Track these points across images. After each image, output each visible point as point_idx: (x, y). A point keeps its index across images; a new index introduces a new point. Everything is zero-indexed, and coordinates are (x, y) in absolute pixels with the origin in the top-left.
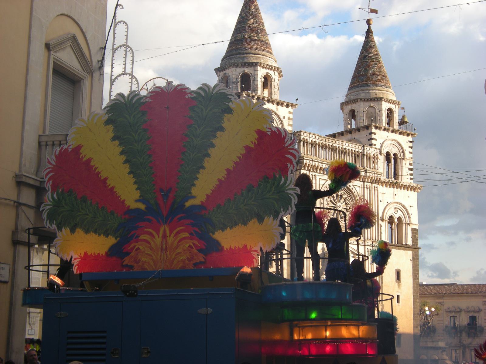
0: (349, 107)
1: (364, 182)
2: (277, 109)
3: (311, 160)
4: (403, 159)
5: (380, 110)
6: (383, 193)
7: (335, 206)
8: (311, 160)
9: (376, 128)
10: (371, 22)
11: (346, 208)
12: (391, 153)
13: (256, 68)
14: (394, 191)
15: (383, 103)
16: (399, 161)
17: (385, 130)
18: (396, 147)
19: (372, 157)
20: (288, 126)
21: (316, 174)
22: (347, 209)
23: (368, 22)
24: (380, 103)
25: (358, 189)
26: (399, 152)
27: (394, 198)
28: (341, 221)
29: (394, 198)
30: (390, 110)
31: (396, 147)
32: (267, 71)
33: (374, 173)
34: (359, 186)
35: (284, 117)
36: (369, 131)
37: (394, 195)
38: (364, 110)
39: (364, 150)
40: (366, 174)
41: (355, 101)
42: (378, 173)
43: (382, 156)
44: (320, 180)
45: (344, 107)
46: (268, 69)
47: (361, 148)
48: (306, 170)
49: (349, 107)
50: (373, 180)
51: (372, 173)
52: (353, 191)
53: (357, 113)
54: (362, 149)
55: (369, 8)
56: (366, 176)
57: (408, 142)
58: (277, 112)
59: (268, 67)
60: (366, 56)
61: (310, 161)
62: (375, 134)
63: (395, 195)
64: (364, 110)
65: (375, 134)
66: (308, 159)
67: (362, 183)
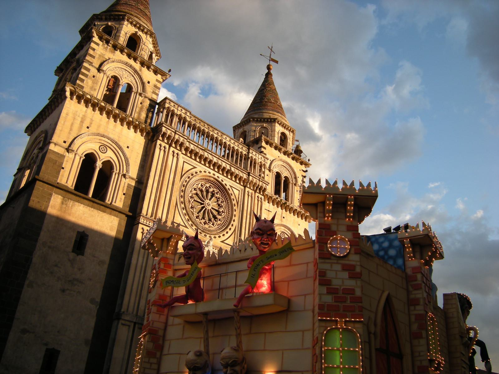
0: (241, 130)
1: (245, 187)
2: (141, 70)
3: (173, 132)
4: (295, 185)
5: (273, 131)
6: (269, 211)
7: (203, 202)
8: (173, 132)
9: (267, 143)
10: (271, 67)
11: (217, 209)
12: (282, 176)
13: (122, 22)
14: (282, 213)
15: (277, 124)
16: (290, 185)
17: (276, 148)
18: (288, 170)
19: (258, 164)
20: (152, 93)
21: (180, 153)
22: (219, 212)
23: (269, 68)
24: (273, 124)
25: (236, 192)
26: (290, 177)
27: (282, 221)
28: (209, 224)
29: (282, 221)
30: (283, 134)
31: (288, 170)
32: (137, 30)
33: (259, 179)
34: (239, 191)
35: (149, 82)
36: (259, 146)
37: (281, 217)
38: (255, 129)
39: (248, 153)
40: (248, 178)
41: (247, 121)
42: (263, 181)
43: (271, 173)
44: (185, 163)
45: (236, 132)
46: (139, 28)
47: (246, 150)
48: (166, 143)
49: (241, 130)
50: (257, 188)
51: (256, 179)
52: (230, 192)
53: (248, 132)
54: (247, 151)
55: (270, 57)
56: (249, 180)
57: (301, 170)
58: (140, 72)
59: (138, 25)
60: (264, 89)
61: (173, 133)
62: (265, 148)
63: (284, 218)
64: (255, 129)
65: (265, 148)
66: (170, 128)
67: (243, 188)
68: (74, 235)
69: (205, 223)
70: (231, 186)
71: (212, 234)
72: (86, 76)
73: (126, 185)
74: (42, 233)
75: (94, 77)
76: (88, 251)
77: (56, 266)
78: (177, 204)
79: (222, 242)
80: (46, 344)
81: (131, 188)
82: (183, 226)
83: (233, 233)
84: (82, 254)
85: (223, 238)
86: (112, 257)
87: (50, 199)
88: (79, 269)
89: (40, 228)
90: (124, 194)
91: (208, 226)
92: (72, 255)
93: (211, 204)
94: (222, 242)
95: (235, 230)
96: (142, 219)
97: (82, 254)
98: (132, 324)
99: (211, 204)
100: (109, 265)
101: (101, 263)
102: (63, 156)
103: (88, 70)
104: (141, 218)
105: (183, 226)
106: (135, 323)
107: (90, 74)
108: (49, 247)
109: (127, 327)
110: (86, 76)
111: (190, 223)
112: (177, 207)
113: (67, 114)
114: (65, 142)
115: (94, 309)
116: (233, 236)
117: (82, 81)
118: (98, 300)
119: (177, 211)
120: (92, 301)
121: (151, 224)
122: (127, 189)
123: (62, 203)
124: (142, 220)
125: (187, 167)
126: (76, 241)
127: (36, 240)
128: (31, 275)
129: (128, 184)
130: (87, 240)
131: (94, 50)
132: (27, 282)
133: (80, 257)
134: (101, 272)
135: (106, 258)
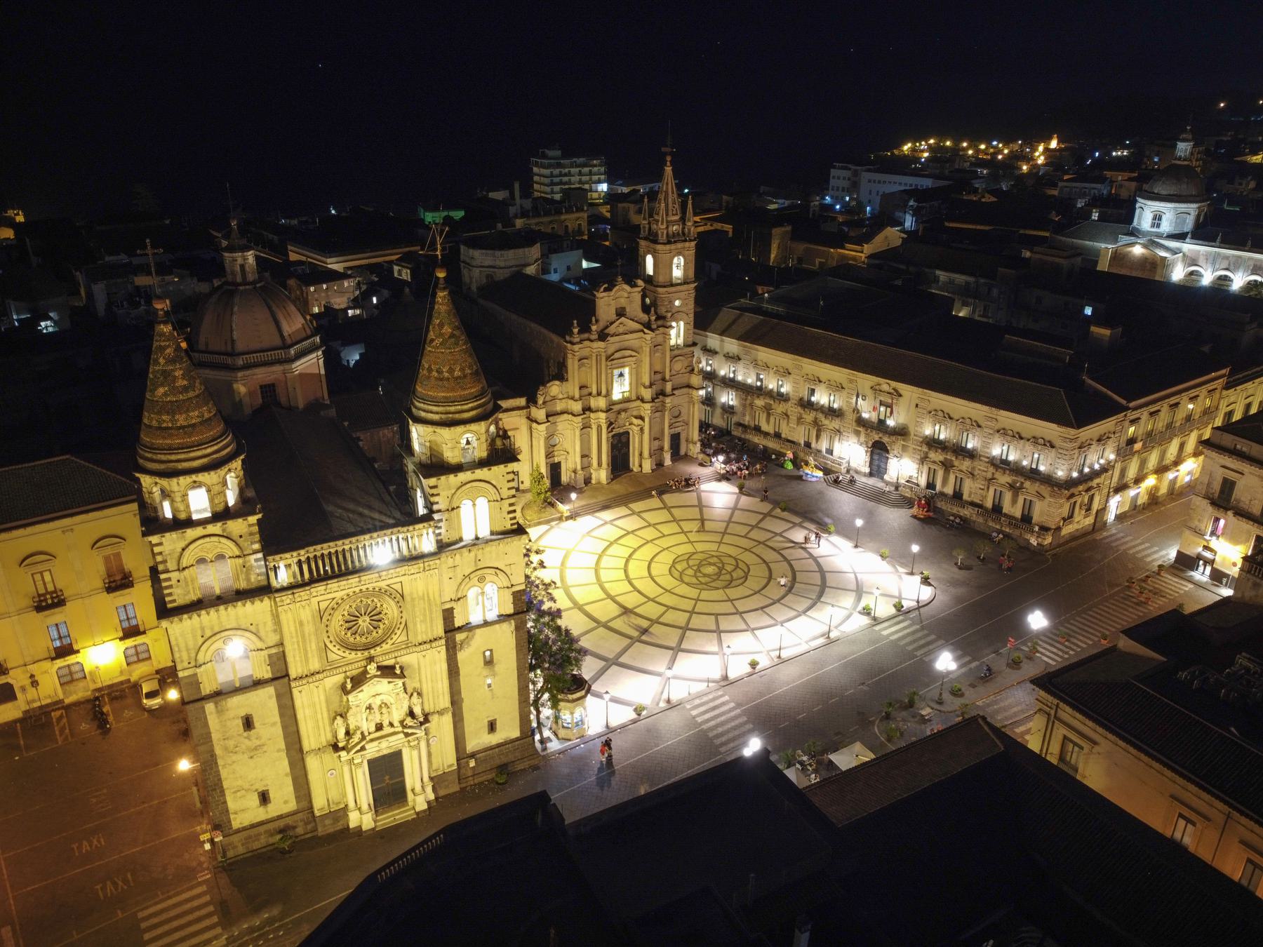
68: (240, 722)
70: (388, 586)
72: (170, 587)
73: (267, 657)
74: (213, 735)
75: (179, 581)
76: (257, 724)
77: (237, 747)
79: (393, 644)
80: (256, 790)
84: (254, 728)
86: (282, 715)
87: (204, 712)
88: (257, 738)
89: (210, 733)
92: (245, 734)
93: (364, 622)
97: (254, 728)
99: (364, 622)
100: (281, 722)
101: (274, 724)
102: (195, 675)
103: (169, 579)
107: (173, 582)
108: (224, 739)
110: (170, 587)
111: (348, 652)
113: (176, 640)
114: (189, 663)
115: (284, 754)
117: (170, 594)
118: (284, 747)
119: (329, 652)
120: (279, 751)
123: (216, 707)
125: (323, 605)
126: (243, 724)
127: (211, 741)
128: (220, 762)
130: (252, 718)
131: (161, 553)
132: (220, 768)
133: (253, 731)
134: (278, 731)
135: (277, 719)
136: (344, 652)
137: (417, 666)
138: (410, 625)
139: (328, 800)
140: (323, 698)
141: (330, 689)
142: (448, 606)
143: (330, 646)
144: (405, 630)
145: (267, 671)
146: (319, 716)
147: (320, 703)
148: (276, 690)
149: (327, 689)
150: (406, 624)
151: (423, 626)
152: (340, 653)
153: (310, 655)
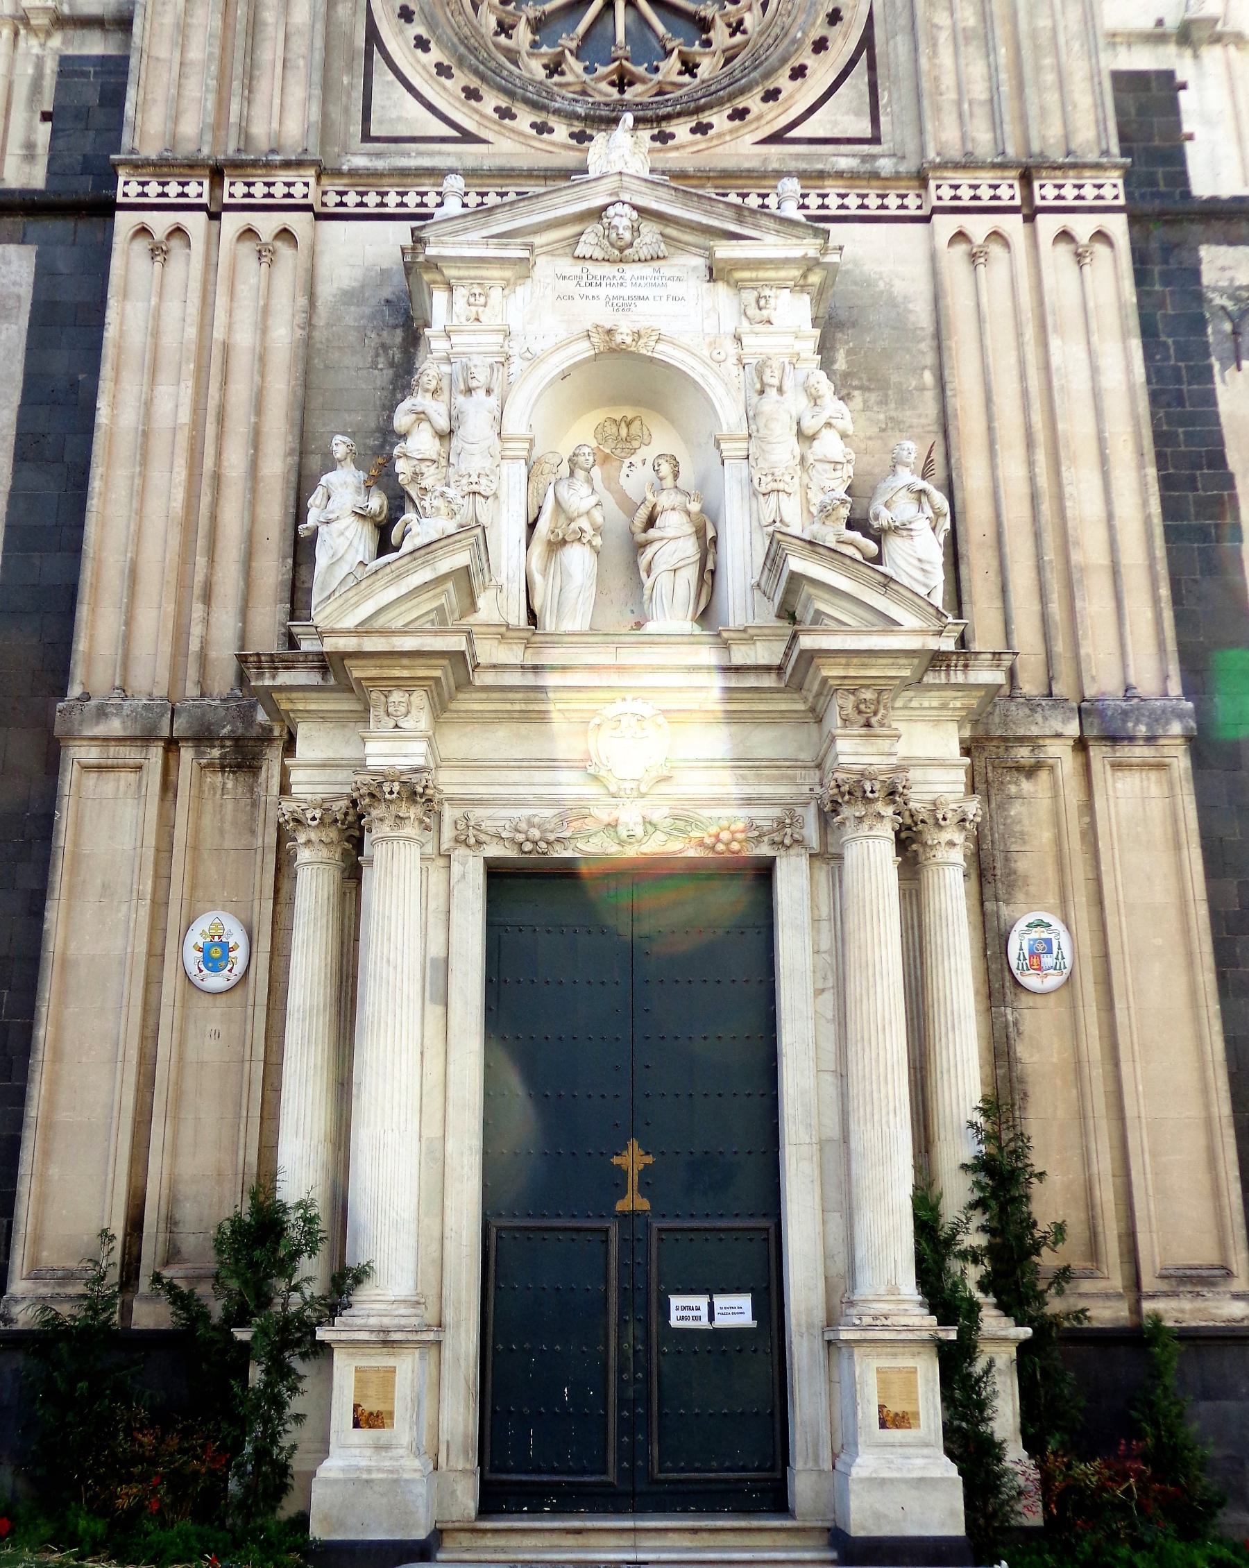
69: (623, 81)
71: (668, 117)
73: (51, 67)
78: (373, 35)
79: (776, 138)
81: (85, 74)
82: (443, 140)
83: (852, 63)
85: (775, 117)
90: (46, 117)
91: (651, 87)
94: (776, 138)
95: (867, 42)
96: (126, 183)
98: (156, 755)
104: (121, 180)
105: (443, 140)
106: (172, 745)
109: (132, 777)
111: (491, 101)
112: (377, 56)
116: (859, 78)
119: (382, 76)
121: (192, 189)
122: (60, 87)
124: (134, 189)
129: (64, 60)
136: (472, 94)
137: (921, 314)
138: (892, 48)
139: (135, 1224)
140: (283, 334)
141: (350, 297)
142: (1143, 60)
143: (396, 40)
144: (859, 78)
145: (30, 146)
146: (235, 460)
147: (262, 359)
148: (44, 273)
149: (326, 291)
150: (867, 42)
151: (977, 70)
152: (446, 95)
153: (270, 53)
